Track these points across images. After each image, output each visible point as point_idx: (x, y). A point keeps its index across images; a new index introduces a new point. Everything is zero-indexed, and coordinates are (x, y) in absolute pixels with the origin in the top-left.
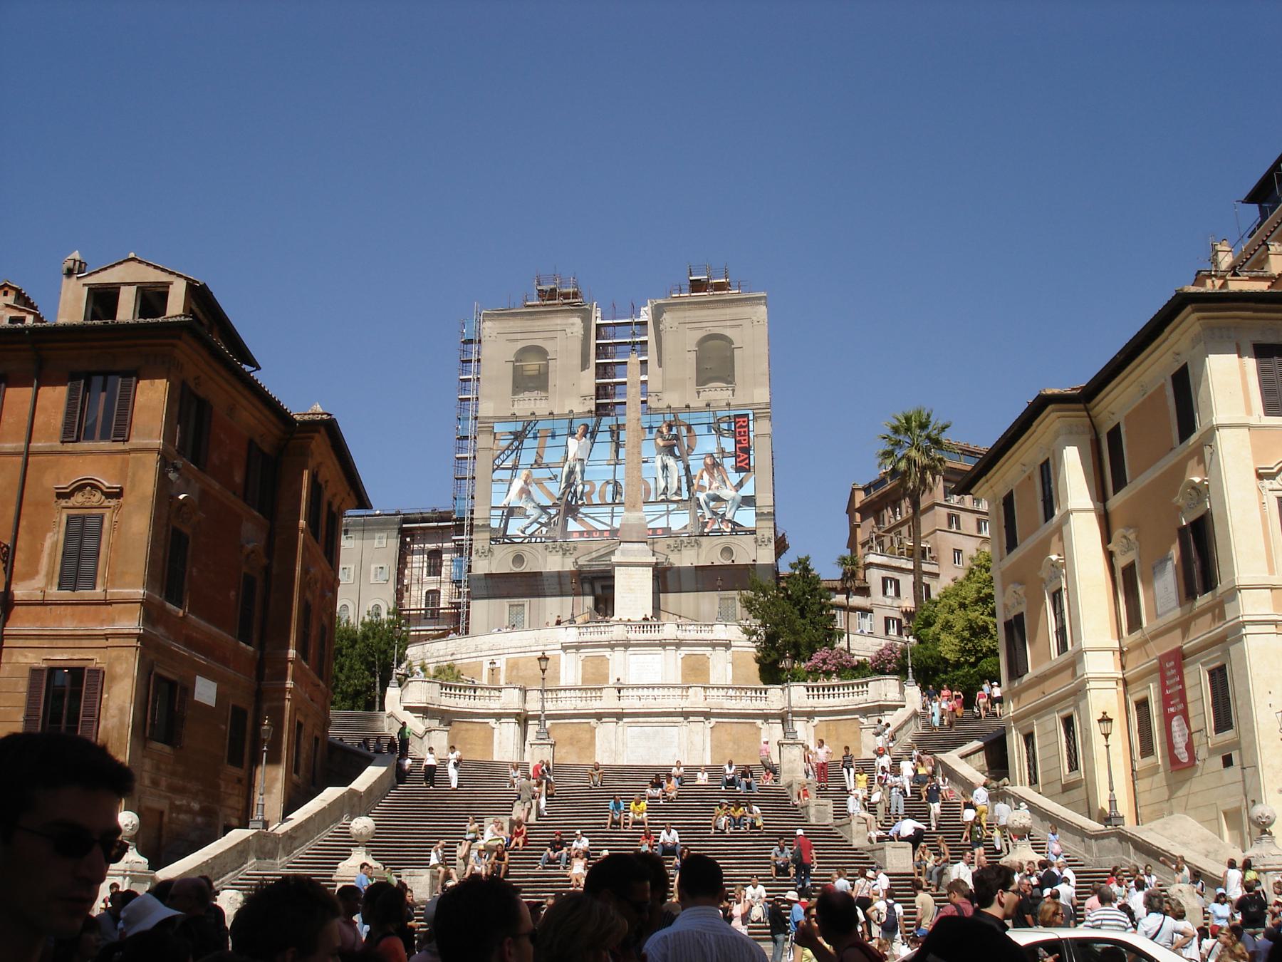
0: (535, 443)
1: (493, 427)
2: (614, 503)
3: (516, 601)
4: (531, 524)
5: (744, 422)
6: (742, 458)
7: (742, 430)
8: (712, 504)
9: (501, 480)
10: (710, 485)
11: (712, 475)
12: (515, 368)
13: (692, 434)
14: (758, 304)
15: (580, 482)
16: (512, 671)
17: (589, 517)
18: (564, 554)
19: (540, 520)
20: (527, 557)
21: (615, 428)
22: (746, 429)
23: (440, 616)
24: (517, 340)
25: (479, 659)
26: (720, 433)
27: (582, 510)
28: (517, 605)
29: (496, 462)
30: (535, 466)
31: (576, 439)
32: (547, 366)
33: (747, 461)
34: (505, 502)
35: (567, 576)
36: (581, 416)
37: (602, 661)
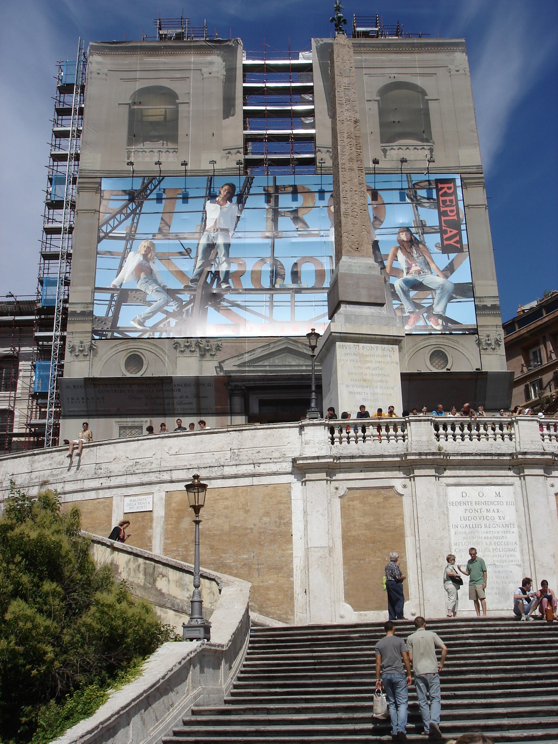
0: (160, 207)
1: (100, 184)
2: (272, 288)
3: (129, 421)
4: (154, 313)
5: (449, 188)
6: (449, 234)
7: (448, 198)
8: (412, 293)
9: (110, 253)
10: (408, 269)
11: (409, 254)
12: (132, 113)
13: (379, 201)
14: (454, 51)
15: (224, 259)
16: (179, 519)
17: (238, 306)
18: (202, 356)
19: (166, 308)
20: (147, 357)
21: (271, 190)
22: (453, 198)
23: (14, 447)
24: (135, 79)
25: (102, 494)
26: (417, 202)
27: (228, 296)
28: (130, 428)
29: (104, 228)
30: (159, 236)
31: (218, 203)
32: (176, 112)
33: (457, 238)
34: (115, 282)
35: (209, 385)
36: (224, 174)
37: (386, 498)
